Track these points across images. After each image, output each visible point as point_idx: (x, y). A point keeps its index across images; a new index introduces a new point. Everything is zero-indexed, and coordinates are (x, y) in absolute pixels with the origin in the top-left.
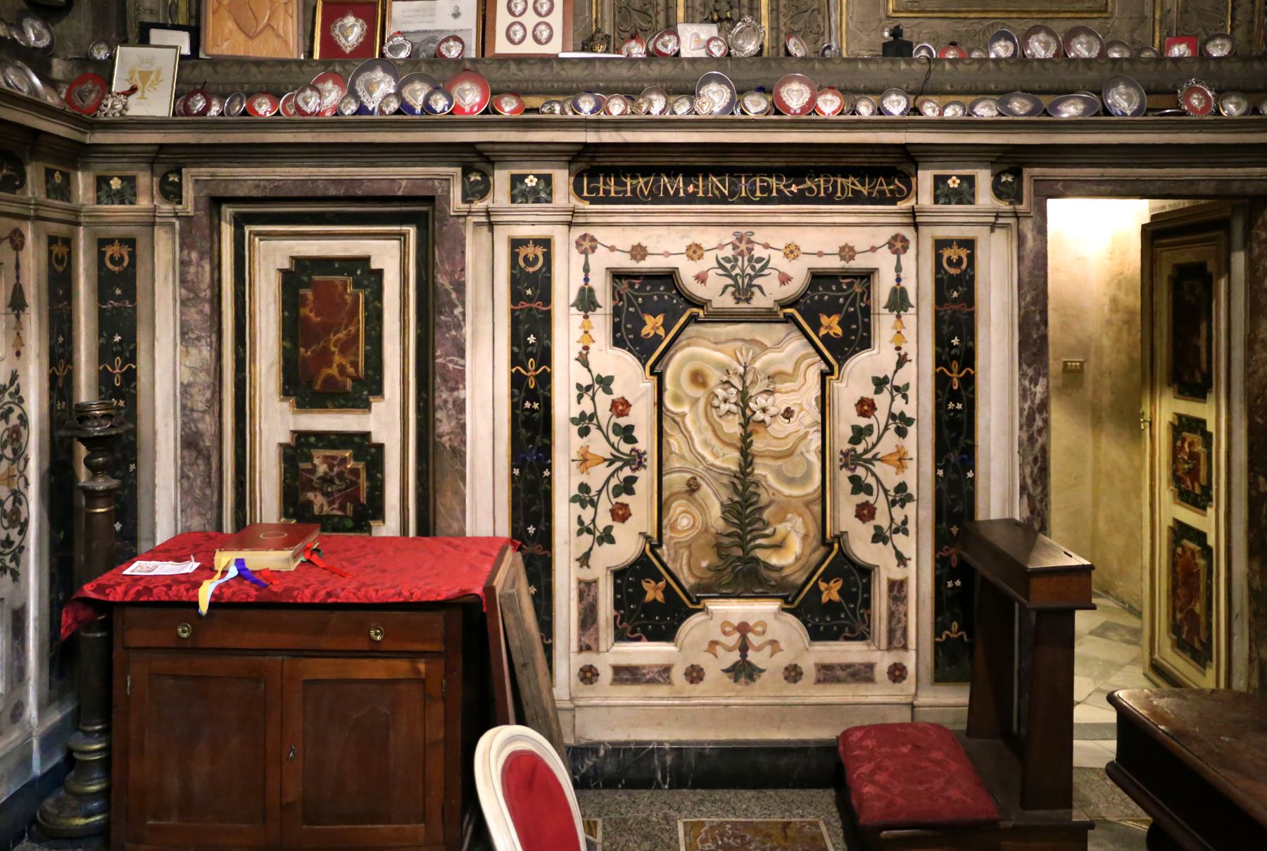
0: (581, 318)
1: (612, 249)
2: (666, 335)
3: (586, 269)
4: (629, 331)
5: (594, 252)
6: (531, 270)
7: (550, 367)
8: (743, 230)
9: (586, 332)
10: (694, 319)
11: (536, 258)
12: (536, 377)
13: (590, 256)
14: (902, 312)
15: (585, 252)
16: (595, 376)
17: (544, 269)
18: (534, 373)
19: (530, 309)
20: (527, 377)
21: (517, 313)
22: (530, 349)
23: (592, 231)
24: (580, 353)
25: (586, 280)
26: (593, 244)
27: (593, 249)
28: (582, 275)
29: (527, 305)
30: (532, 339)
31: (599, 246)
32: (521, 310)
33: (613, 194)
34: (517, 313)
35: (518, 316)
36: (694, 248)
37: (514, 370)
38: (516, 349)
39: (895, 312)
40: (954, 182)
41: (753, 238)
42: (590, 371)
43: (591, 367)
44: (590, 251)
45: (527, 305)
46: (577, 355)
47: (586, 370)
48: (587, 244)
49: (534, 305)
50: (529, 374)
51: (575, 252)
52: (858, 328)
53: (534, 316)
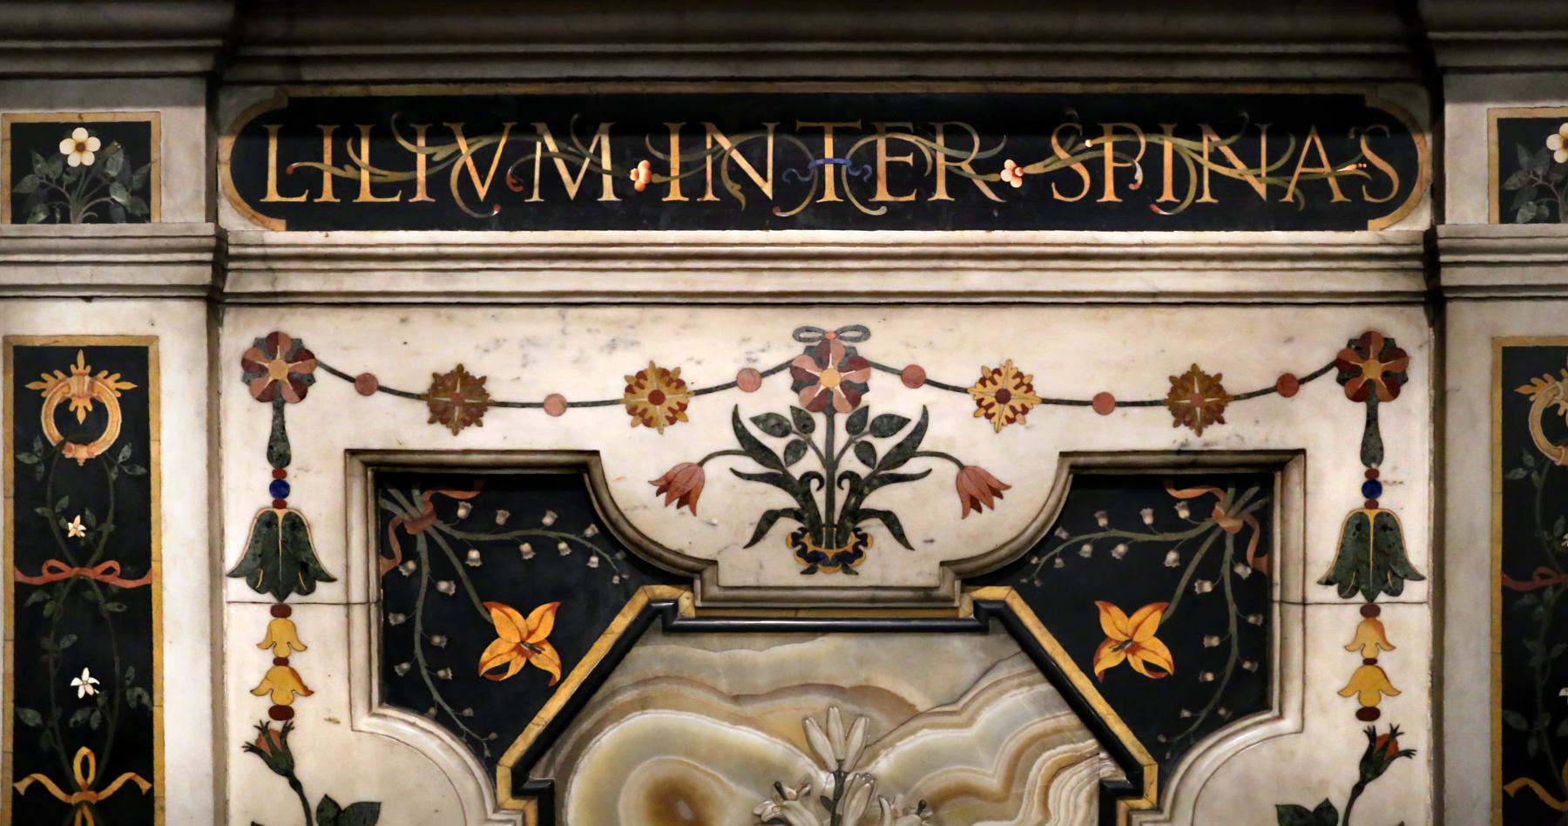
0: (265, 615)
1: (366, 385)
2: (564, 677)
3: (279, 453)
4: (437, 658)
5: (302, 396)
6: (82, 453)
7: (148, 774)
8: (828, 321)
9: (281, 662)
10: (658, 621)
11: (99, 412)
12: (100, 808)
13: (290, 410)
14: (1382, 597)
15: (272, 396)
16: (314, 803)
17: (126, 452)
18: (92, 797)
19: (82, 584)
20: (68, 809)
21: (35, 597)
22: (79, 716)
23: (298, 325)
24: (263, 729)
25: (280, 489)
26: (300, 367)
27: (301, 386)
28: (265, 474)
29: (69, 572)
30: (85, 684)
31: (319, 374)
32: (49, 587)
33: (365, 195)
34: (35, 597)
35: (39, 606)
36: (652, 384)
37: (22, 786)
38: (32, 717)
39: (1360, 598)
40: (80, 148)
41: (864, 350)
42: (296, 785)
43: (301, 772)
44: (288, 390)
45: (69, 572)
46: (252, 736)
47: (283, 782)
48: (279, 369)
49: (93, 573)
50: (75, 798)
51: (237, 395)
52: (1225, 647)
53: (95, 605)
